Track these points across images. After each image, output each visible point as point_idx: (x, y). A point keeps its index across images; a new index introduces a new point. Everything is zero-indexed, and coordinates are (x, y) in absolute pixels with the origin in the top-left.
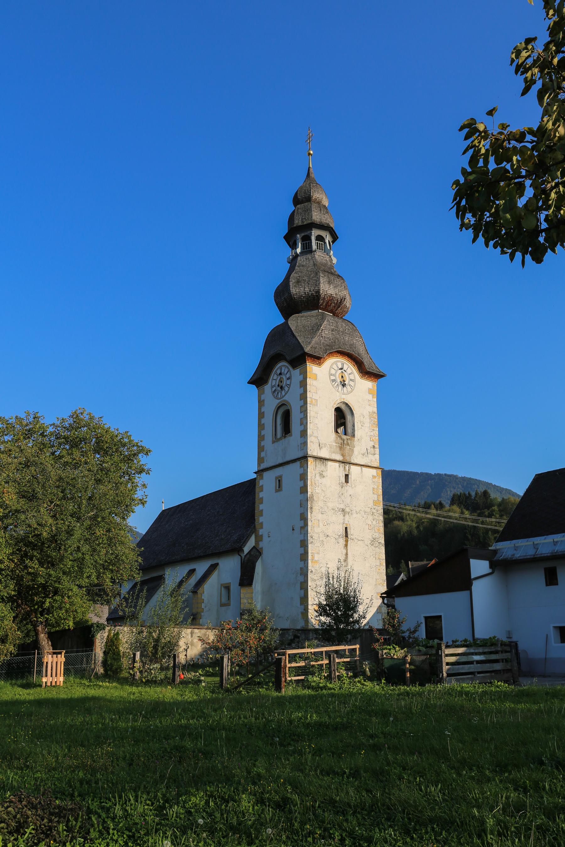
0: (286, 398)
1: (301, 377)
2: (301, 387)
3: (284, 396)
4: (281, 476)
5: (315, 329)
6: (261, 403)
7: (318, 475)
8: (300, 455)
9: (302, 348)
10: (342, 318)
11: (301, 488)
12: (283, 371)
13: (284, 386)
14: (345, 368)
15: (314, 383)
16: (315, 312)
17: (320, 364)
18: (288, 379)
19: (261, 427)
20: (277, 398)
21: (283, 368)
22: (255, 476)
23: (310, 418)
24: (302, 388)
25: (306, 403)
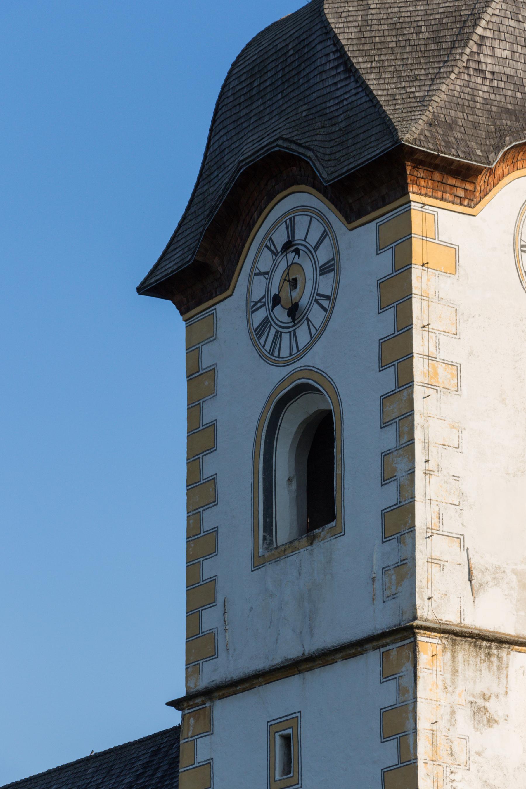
0: (315, 358)
1: (384, 263)
2: (382, 308)
3: (309, 347)
4: (294, 719)
5: (448, 35)
6: (201, 381)
7: (464, 716)
8: (381, 620)
9: (388, 128)
11: (385, 772)
12: (299, 235)
13: (304, 302)
17: (471, 201)
18: (325, 269)
19: (201, 491)
20: (271, 357)
21: (302, 221)
22: (173, 718)
23: (426, 450)
24: (390, 314)
25: (405, 382)
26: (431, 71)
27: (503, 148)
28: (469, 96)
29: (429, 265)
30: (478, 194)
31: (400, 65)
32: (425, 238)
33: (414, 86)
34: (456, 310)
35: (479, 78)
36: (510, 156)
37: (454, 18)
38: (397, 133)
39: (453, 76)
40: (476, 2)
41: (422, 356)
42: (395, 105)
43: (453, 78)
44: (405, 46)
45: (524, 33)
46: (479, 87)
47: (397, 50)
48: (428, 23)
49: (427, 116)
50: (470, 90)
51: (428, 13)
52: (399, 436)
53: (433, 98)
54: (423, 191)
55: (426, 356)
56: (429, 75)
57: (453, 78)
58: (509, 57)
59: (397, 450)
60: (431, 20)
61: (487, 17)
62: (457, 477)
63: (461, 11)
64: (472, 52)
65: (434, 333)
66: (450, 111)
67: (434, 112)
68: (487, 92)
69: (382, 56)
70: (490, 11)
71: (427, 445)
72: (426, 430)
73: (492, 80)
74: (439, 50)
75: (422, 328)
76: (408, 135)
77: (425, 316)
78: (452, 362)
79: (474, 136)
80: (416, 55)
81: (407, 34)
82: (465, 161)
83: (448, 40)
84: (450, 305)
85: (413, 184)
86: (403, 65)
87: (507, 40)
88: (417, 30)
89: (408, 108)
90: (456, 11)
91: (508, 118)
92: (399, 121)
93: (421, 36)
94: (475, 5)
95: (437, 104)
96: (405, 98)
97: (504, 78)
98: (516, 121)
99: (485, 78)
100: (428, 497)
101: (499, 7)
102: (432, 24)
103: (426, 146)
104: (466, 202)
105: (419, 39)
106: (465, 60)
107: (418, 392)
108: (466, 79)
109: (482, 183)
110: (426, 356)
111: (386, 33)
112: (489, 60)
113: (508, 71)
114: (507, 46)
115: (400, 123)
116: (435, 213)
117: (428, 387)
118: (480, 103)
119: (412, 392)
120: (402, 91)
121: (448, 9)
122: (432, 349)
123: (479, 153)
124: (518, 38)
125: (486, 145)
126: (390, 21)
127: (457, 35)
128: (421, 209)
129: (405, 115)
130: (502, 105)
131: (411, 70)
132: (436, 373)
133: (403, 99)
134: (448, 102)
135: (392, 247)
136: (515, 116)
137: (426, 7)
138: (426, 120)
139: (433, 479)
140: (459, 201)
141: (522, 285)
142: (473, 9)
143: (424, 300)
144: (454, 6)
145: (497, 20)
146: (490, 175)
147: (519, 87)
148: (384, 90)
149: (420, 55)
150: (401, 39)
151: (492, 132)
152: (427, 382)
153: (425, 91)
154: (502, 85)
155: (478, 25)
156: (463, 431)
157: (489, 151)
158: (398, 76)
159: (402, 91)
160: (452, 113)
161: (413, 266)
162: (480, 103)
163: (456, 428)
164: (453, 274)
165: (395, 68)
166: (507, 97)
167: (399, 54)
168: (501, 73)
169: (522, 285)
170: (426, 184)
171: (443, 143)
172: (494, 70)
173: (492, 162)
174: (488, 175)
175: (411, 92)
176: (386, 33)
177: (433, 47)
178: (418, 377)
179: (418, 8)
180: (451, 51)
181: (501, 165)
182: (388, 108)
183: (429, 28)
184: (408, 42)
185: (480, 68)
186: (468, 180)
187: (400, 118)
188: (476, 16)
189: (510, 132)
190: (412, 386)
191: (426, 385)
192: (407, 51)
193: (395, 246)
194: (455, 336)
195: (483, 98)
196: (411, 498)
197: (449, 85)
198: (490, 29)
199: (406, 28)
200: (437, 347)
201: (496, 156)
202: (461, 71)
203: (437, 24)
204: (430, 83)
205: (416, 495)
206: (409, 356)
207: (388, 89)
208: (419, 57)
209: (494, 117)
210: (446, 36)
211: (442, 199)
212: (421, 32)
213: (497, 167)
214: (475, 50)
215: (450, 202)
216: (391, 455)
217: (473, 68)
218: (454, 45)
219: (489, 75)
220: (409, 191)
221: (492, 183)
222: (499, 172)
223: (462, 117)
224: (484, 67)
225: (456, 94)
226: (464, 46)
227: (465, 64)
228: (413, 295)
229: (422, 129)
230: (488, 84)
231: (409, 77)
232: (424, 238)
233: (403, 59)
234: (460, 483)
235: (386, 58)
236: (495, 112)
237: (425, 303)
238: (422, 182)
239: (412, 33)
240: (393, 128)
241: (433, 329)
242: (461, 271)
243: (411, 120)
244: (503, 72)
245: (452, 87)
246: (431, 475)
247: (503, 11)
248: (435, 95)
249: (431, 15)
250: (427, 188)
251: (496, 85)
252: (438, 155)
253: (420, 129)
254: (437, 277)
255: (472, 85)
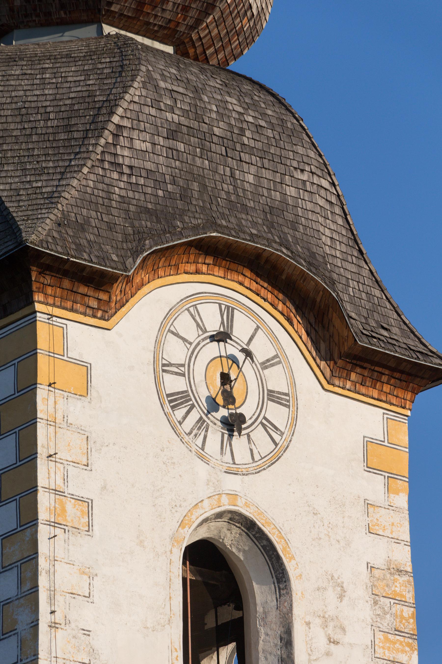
5: (80, 123)
9: (11, 228)
10: (222, 67)
14: (242, 327)
15: (75, 410)
16: (79, 37)
23: (52, 599)
26: (61, 164)
27: (142, 253)
28: (104, 193)
29: (56, 385)
30: (113, 305)
31: (24, 156)
32: (52, 355)
33: (40, 180)
34: (87, 437)
35: (115, 172)
36: (150, 262)
37: (87, 104)
38: (21, 233)
39: (85, 170)
40: (112, 87)
41: (48, 490)
42: (19, 201)
43: (85, 172)
44: (31, 135)
45: (166, 123)
46: (115, 183)
47: (21, 139)
48: (57, 109)
49: (56, 214)
50: (105, 186)
51: (57, 98)
52: (20, 582)
53: (63, 195)
54: (51, 300)
55: (53, 490)
56: (58, 168)
57: (85, 172)
58: (150, 148)
59: (18, 599)
60: (60, 105)
61: (125, 105)
62: (87, 631)
63: (95, 96)
64: (107, 143)
65: (62, 463)
66: (82, 210)
67: (63, 210)
68: (124, 189)
69: (4, 145)
70: (128, 97)
71: (52, 593)
72: (52, 576)
73: (130, 175)
74: (69, 140)
75: (48, 457)
76: (34, 237)
77: (52, 444)
78: (82, 497)
79: (109, 239)
80: (43, 145)
81: (33, 121)
82: (98, 266)
83: (80, 129)
84: (81, 432)
85: (39, 292)
86: (28, 156)
87: (147, 130)
88: (45, 116)
89: (34, 205)
90: (89, 96)
91: (148, 219)
92: (23, 220)
93: (49, 124)
94: (111, 91)
95: (67, 202)
96: (30, 194)
97: (144, 173)
98: (157, 222)
99: (122, 173)
100: (54, 654)
101: (138, 93)
102: (62, 110)
103: (54, 249)
104: (99, 314)
105: (47, 127)
106: (99, 152)
107: (43, 532)
108: (101, 174)
109: (118, 292)
110: (53, 490)
111: (10, 119)
112: (126, 153)
113: (149, 165)
114: (148, 137)
115: (24, 222)
116: (65, 326)
117: (54, 526)
118: (116, 201)
119: (36, 532)
120: (27, 186)
121: (80, 94)
122: (60, 482)
123: (114, 258)
124: (160, 128)
125: (123, 249)
126: (14, 106)
127: (90, 123)
128: (47, 321)
129: (30, 213)
130: (141, 203)
131: (38, 162)
132: (64, 510)
133: (28, 195)
134: (80, 199)
135: (14, 364)
136: (157, 217)
137: (55, 91)
138: (54, 219)
139: (60, 633)
140: (91, 313)
141: (163, 410)
142: (109, 95)
143: (50, 425)
144: (87, 91)
145: (136, 107)
146: (127, 284)
147: (161, 184)
148: (6, 184)
149: (48, 146)
150: (26, 126)
151: (130, 235)
152: (53, 520)
153: (54, 186)
154: (142, 181)
155: (115, 113)
156: (95, 578)
157: (126, 257)
158: (23, 168)
159: (27, 186)
160: (85, 212)
161: (38, 386)
162: (116, 201)
163: (87, 575)
164: (84, 396)
165: (19, 159)
166: (147, 195)
167: (24, 144)
168: (140, 168)
169: (163, 410)
170: (53, 292)
171: (74, 247)
172: (133, 165)
173: (129, 268)
174: (125, 283)
175: (37, 187)
176: (10, 119)
177: (62, 136)
178: (43, 515)
179: (46, 92)
180: (83, 142)
181: (140, 273)
182: (11, 205)
183: (59, 115)
184: (34, 130)
185: (116, 162)
186: (102, 288)
187: (25, 216)
188: (113, 103)
189: (150, 235)
190: (36, 525)
191: (53, 524)
192: (33, 140)
193: (18, 362)
194: (86, 468)
195: (119, 195)
196: (34, 655)
197: (81, 180)
198: (128, 118)
199: (32, 114)
200: (65, 479)
201: (134, 262)
202: (94, 164)
203: (68, 111)
204: (59, 177)
205: (40, 652)
206: (33, 490)
207: (11, 183)
208: (46, 147)
209: (133, 217)
210: (77, 124)
211: (72, 310)
212: (49, 119)
213: (135, 275)
214: (110, 141)
215: (81, 313)
216: (12, 603)
217: (108, 161)
218: (87, 134)
219: (126, 170)
220: (34, 299)
221: (130, 292)
222: (137, 280)
223: (96, 217)
224: (121, 161)
225: (89, 190)
226: (99, 137)
227: (99, 157)
228: (38, 420)
229: (49, 229)
230: (126, 180)
231: (35, 170)
232: (51, 354)
233: (29, 149)
234: (91, 638)
235: (10, 148)
236: (133, 212)
237: (51, 429)
238: (49, 290)
239: (39, 120)
240: (16, 228)
241: (61, 459)
242: (93, 393)
243: (37, 218)
244: (143, 167)
245: (84, 182)
246: (57, 628)
247: (143, 98)
248: (65, 191)
249: (60, 100)
250: (55, 297)
251: (134, 182)
252: (68, 259)
253: (47, 229)
254: (65, 399)
255: (106, 180)
